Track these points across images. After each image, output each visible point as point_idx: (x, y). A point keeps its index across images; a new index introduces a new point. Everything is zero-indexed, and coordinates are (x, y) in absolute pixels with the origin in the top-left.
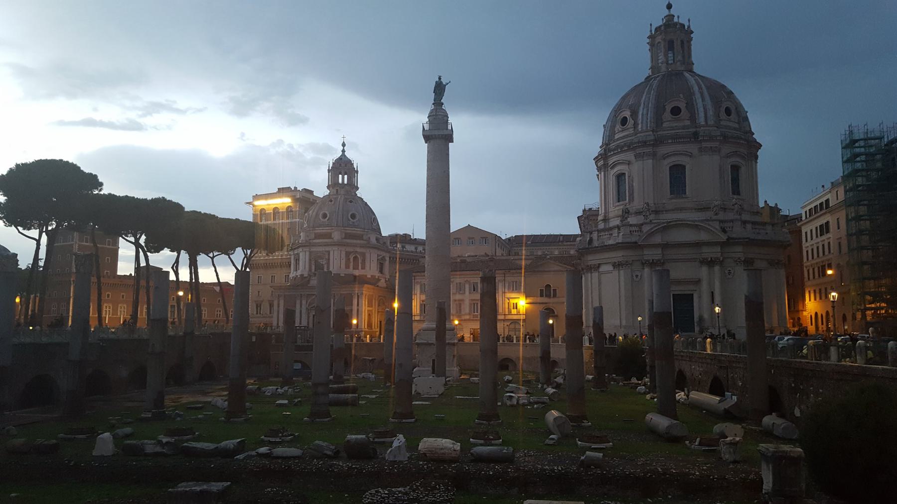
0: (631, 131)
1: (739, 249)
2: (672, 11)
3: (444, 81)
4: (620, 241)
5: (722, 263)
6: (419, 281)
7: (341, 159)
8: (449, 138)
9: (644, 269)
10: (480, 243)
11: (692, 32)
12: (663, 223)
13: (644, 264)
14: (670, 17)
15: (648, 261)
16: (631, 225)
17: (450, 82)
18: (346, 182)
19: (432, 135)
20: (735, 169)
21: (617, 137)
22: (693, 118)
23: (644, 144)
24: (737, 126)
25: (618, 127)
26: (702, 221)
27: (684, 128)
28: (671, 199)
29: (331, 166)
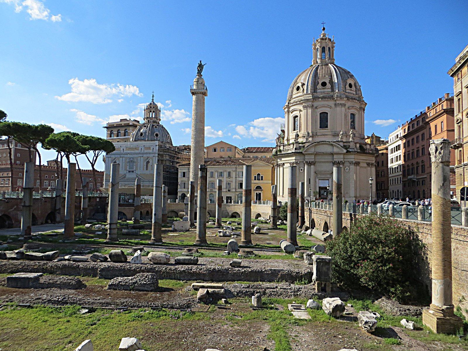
1: (353, 156)
4: (294, 151)
5: (343, 164)
8: (205, 94)
10: (227, 151)
11: (335, 43)
12: (316, 142)
16: (300, 143)
18: (154, 117)
19: (195, 92)
20: (353, 115)
21: (294, 96)
23: (308, 100)
24: (355, 93)
25: (295, 91)
29: (146, 108)
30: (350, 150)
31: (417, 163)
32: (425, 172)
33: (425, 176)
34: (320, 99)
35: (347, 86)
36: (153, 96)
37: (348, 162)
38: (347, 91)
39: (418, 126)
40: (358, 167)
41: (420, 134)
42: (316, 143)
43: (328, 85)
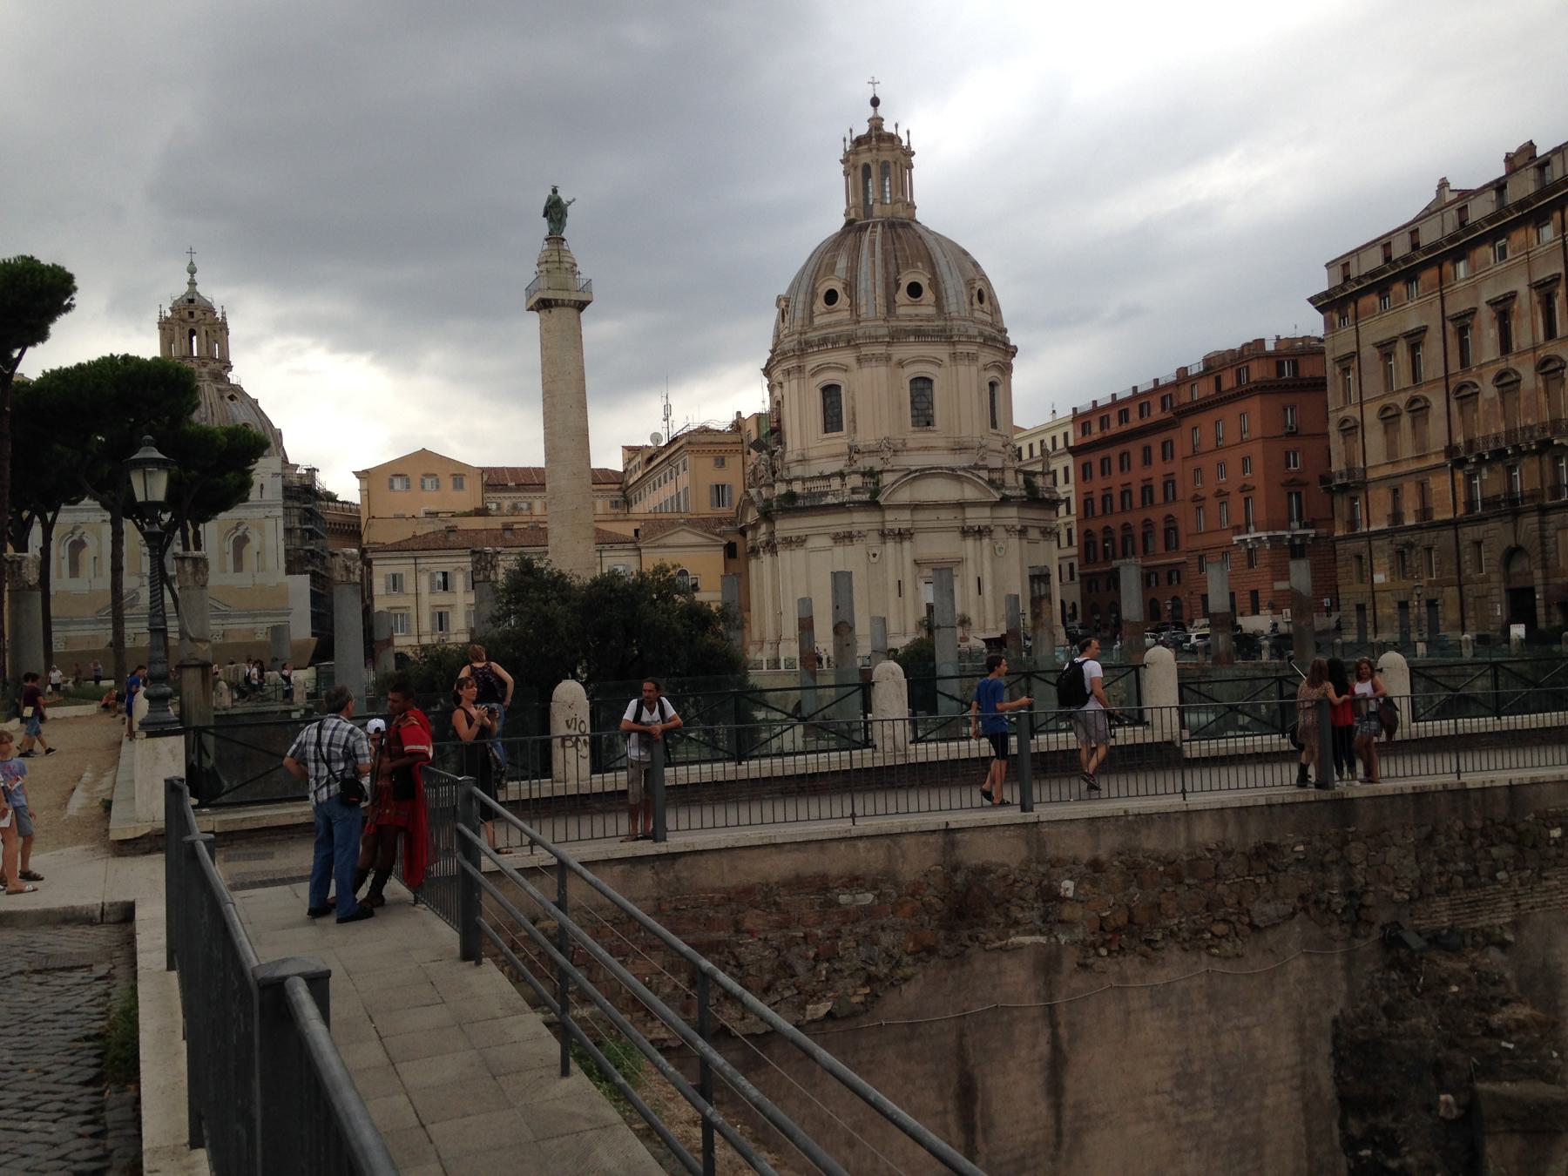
0: (846, 315)
2: (881, 111)
3: (565, 196)
6: (427, 566)
7: (191, 301)
9: (885, 543)
11: (913, 154)
12: (916, 471)
13: (884, 535)
14: (876, 123)
15: (892, 530)
17: (574, 200)
19: (556, 300)
20: (992, 385)
21: (818, 321)
22: (939, 303)
23: (875, 340)
24: (989, 319)
25: (820, 304)
26: (964, 469)
27: (929, 318)
28: (914, 432)
30: (1007, 492)
31: (1147, 523)
32: (1177, 547)
33: (1183, 559)
34: (912, 339)
35: (975, 299)
36: (192, 271)
37: (1003, 529)
38: (978, 314)
39: (1147, 421)
40: (1024, 542)
41: (1155, 442)
42: (918, 474)
43: (928, 295)
